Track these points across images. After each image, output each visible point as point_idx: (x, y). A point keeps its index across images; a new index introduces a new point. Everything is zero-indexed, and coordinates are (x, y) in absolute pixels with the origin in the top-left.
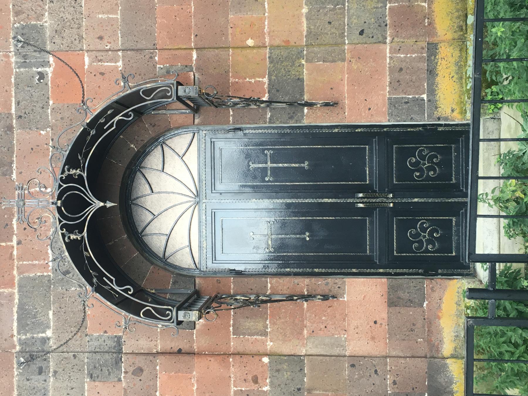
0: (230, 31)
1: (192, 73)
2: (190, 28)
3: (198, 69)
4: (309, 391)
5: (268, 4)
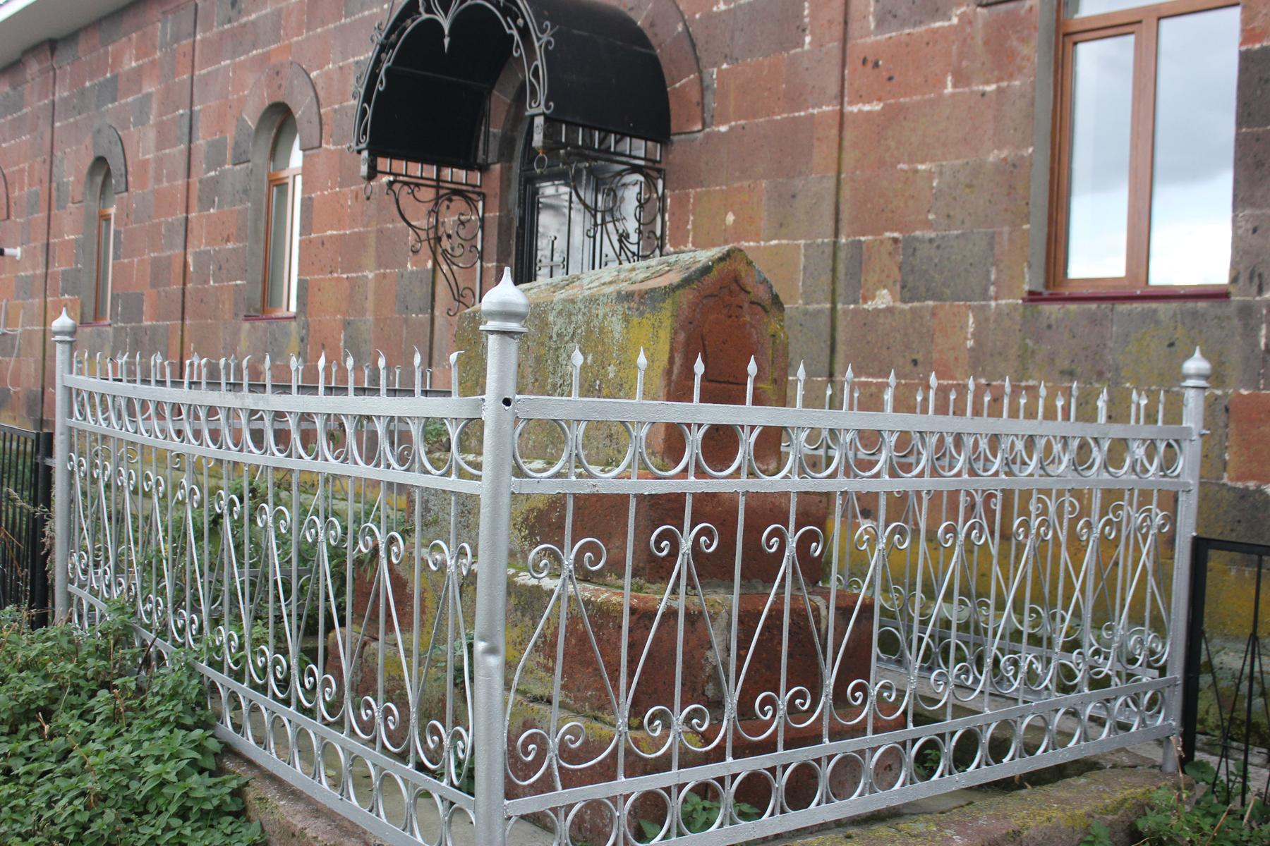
0: (746, 183)
1: (699, 127)
2: (754, 115)
3: (708, 136)
4: (406, 320)
5: (775, 246)
